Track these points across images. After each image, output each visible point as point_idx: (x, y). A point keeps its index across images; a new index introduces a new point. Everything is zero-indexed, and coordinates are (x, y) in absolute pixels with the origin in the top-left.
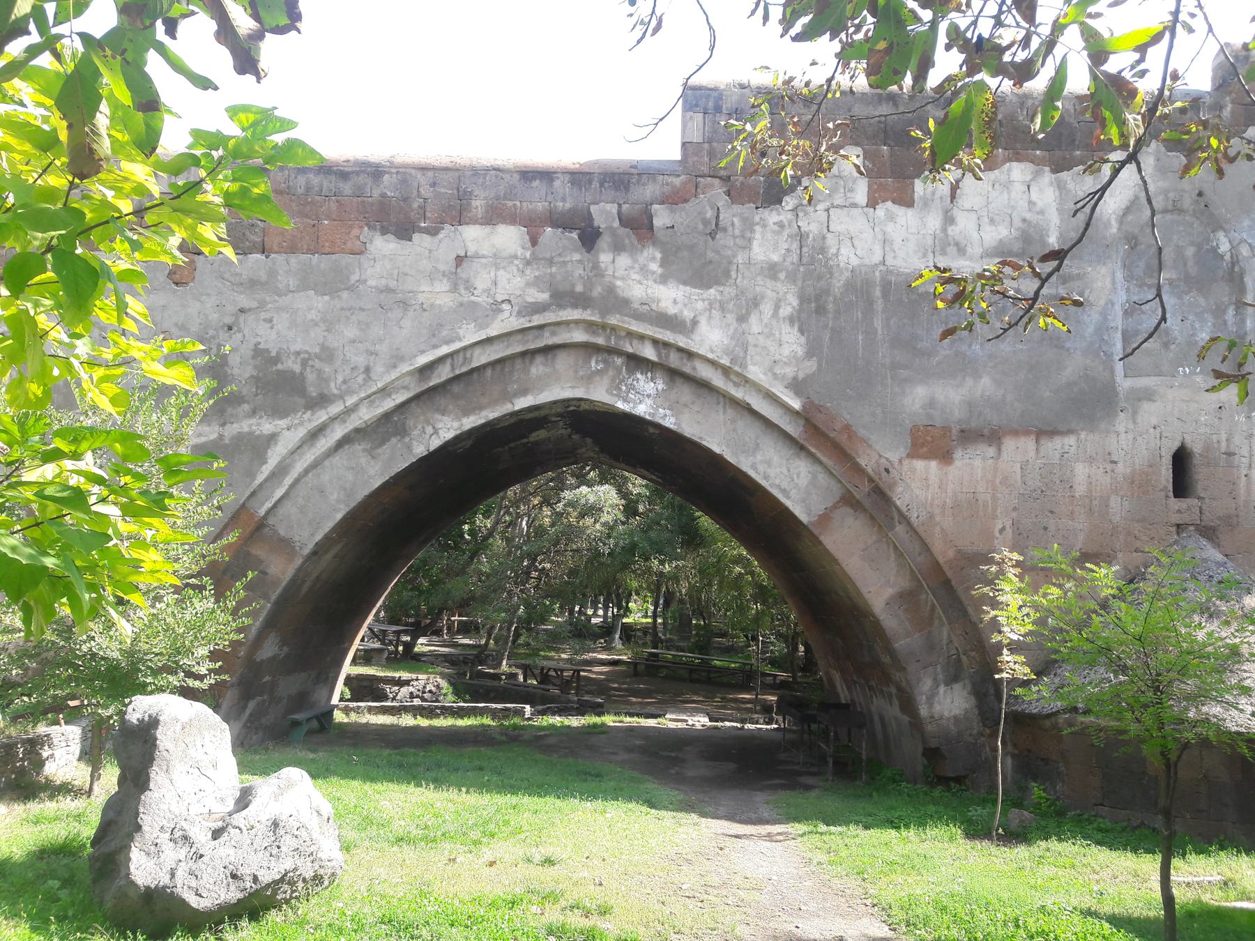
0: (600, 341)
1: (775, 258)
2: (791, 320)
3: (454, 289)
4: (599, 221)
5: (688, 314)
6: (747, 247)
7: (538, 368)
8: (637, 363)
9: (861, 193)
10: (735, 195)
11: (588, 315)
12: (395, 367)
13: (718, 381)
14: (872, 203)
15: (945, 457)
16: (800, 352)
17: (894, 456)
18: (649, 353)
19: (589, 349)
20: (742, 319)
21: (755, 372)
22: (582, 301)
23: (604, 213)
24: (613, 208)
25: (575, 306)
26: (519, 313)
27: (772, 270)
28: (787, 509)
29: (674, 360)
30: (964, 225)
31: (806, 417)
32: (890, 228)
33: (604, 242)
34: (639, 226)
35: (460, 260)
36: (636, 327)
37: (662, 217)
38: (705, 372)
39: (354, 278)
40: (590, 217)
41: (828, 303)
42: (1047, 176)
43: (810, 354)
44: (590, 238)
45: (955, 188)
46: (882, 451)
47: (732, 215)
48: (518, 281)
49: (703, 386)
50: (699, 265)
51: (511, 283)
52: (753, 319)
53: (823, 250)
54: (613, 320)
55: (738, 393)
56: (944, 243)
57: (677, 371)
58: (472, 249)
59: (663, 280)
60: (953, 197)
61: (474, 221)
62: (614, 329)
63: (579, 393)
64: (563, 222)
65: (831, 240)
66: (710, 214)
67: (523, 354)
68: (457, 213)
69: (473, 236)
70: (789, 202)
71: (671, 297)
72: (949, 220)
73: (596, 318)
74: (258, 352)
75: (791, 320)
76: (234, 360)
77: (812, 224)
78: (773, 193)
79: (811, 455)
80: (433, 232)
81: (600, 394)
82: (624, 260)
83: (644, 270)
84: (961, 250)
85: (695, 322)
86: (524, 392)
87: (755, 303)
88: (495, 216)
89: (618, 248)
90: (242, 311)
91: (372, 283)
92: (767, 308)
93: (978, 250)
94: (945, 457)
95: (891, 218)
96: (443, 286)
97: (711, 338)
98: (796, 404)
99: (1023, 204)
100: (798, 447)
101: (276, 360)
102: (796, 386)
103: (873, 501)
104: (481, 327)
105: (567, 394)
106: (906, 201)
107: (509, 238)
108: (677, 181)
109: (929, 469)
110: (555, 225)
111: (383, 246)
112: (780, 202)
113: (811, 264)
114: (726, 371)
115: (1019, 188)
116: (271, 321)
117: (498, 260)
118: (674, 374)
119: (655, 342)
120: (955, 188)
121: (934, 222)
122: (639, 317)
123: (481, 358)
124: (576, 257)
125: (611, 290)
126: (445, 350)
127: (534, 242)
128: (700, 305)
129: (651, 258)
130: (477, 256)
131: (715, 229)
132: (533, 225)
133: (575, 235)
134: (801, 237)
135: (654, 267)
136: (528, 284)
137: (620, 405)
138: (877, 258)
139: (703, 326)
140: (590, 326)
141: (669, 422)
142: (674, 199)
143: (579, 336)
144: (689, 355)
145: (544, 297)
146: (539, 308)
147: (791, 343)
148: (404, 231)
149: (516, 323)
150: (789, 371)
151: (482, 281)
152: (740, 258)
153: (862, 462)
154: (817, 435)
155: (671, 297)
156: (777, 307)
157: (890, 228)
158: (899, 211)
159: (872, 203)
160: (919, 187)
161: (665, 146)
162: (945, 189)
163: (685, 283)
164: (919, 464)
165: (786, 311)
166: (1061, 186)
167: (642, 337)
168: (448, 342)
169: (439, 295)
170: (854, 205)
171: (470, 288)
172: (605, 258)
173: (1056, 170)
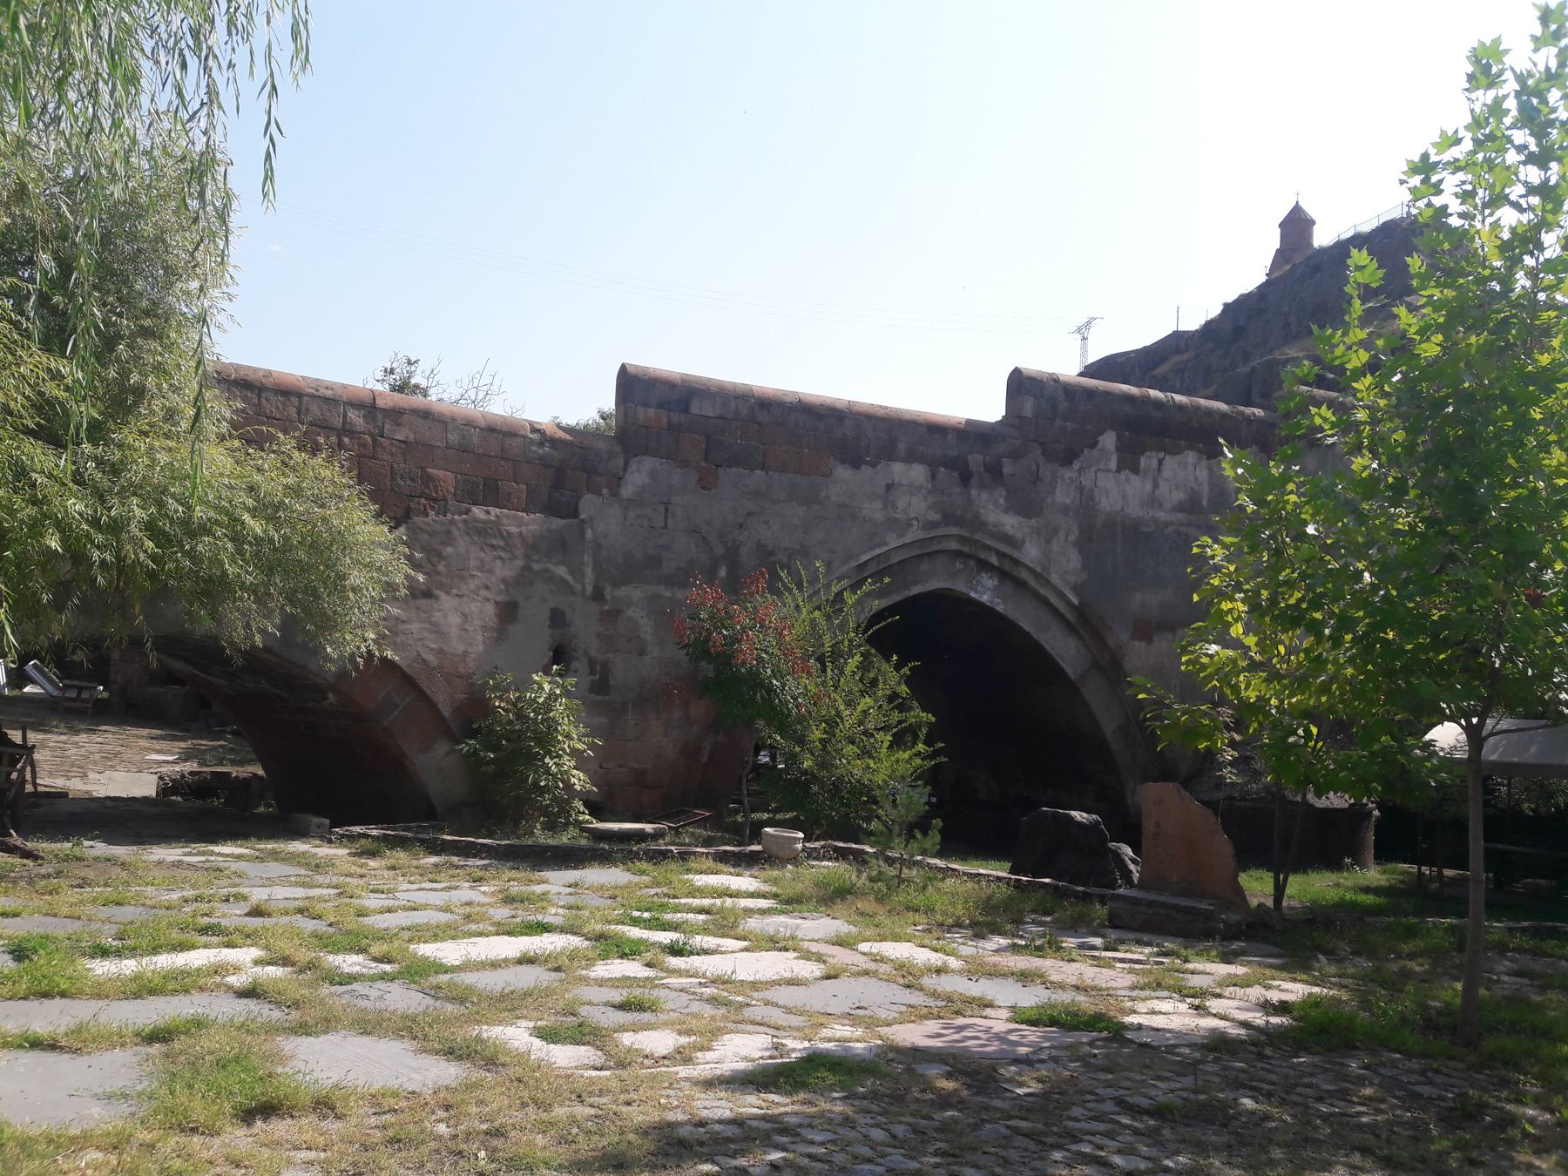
0: (966, 549)
1: (1068, 501)
2: (1075, 544)
3: (885, 507)
4: (973, 467)
5: (1019, 535)
6: (1053, 492)
7: (924, 566)
8: (985, 566)
9: (1113, 465)
10: (1048, 455)
11: (964, 533)
12: (846, 562)
13: (1032, 582)
14: (1119, 470)
15: (1149, 640)
16: (1079, 566)
17: (1124, 637)
18: (994, 560)
19: (958, 554)
20: (1048, 541)
21: (1055, 579)
22: (958, 521)
23: (976, 460)
24: (980, 458)
25: (955, 525)
26: (923, 528)
27: (1065, 510)
28: (1063, 671)
29: (1008, 566)
30: (1163, 488)
31: (1079, 611)
32: (1127, 487)
33: (974, 481)
34: (994, 472)
35: (889, 487)
36: (989, 542)
37: (1008, 469)
38: (1025, 575)
39: (823, 494)
40: (966, 464)
41: (1106, 539)
42: (1204, 462)
43: (1084, 567)
44: (965, 478)
45: (1160, 462)
46: (1119, 635)
47: (1046, 470)
48: (923, 505)
49: (1021, 584)
50: (1026, 505)
51: (916, 506)
52: (1054, 542)
53: (1092, 499)
54: (977, 537)
55: (1043, 591)
56: (1153, 501)
57: (1009, 574)
58: (897, 479)
59: (1006, 511)
60: (1159, 470)
61: (897, 460)
62: (975, 542)
63: (948, 585)
64: (949, 464)
65: (1096, 493)
66: (1034, 468)
67: (922, 556)
68: (888, 452)
69: (897, 468)
70: (1076, 465)
71: (1010, 523)
72: (1156, 485)
73: (966, 534)
74: (760, 547)
75: (1075, 544)
76: (744, 551)
77: (1087, 481)
78: (1068, 458)
79: (1081, 638)
80: (873, 465)
81: (960, 586)
82: (985, 495)
83: (996, 503)
84: (1161, 505)
85: (1023, 541)
86: (916, 583)
87: (1056, 531)
88: (911, 457)
89: (982, 487)
90: (749, 514)
91: (833, 499)
92: (1062, 535)
93: (1168, 506)
94: (1149, 640)
95: (1128, 481)
96: (878, 505)
97: (1031, 553)
98: (1076, 601)
99: (1192, 478)
100: (1070, 628)
101: (771, 553)
102: (1076, 589)
103: (1111, 668)
104: (901, 535)
105: (941, 585)
106: (1136, 471)
107: (918, 473)
108: (1017, 443)
109: (1139, 646)
110: (946, 467)
111: (843, 472)
112: (1071, 463)
113: (1086, 505)
114: (1036, 575)
115: (1190, 467)
116: (767, 523)
117: (913, 489)
118: (1003, 575)
119: (1000, 554)
120: (1160, 462)
121: (1148, 486)
122: (993, 536)
123: (896, 558)
124: (958, 490)
125: (977, 515)
126: (878, 551)
127: (933, 477)
128: (1026, 530)
129: (1000, 495)
130: (899, 484)
131: (1037, 478)
132: (933, 464)
133: (956, 475)
134: (1081, 488)
135: (1001, 501)
136: (929, 507)
137: (973, 595)
138: (1119, 507)
139: (1028, 545)
140: (961, 539)
141: (1000, 608)
142: (1016, 455)
143: (954, 546)
144: (1016, 562)
145: (938, 517)
146: (934, 525)
147: (1073, 560)
148: (856, 464)
149: (921, 534)
150: (1073, 579)
151: (901, 504)
152: (1049, 500)
153: (1111, 642)
154: (1084, 623)
155: (1010, 523)
156: (1067, 536)
157: (1127, 487)
158: (1133, 477)
159: (1119, 470)
160: (1143, 461)
161: (990, 407)
162: (1155, 463)
163: (1018, 513)
164: (1136, 643)
165: (1072, 538)
166: (1210, 470)
167: (990, 549)
168: (880, 545)
169: (874, 510)
170: (1109, 470)
171: (894, 507)
172: (974, 492)
173: (1209, 458)
